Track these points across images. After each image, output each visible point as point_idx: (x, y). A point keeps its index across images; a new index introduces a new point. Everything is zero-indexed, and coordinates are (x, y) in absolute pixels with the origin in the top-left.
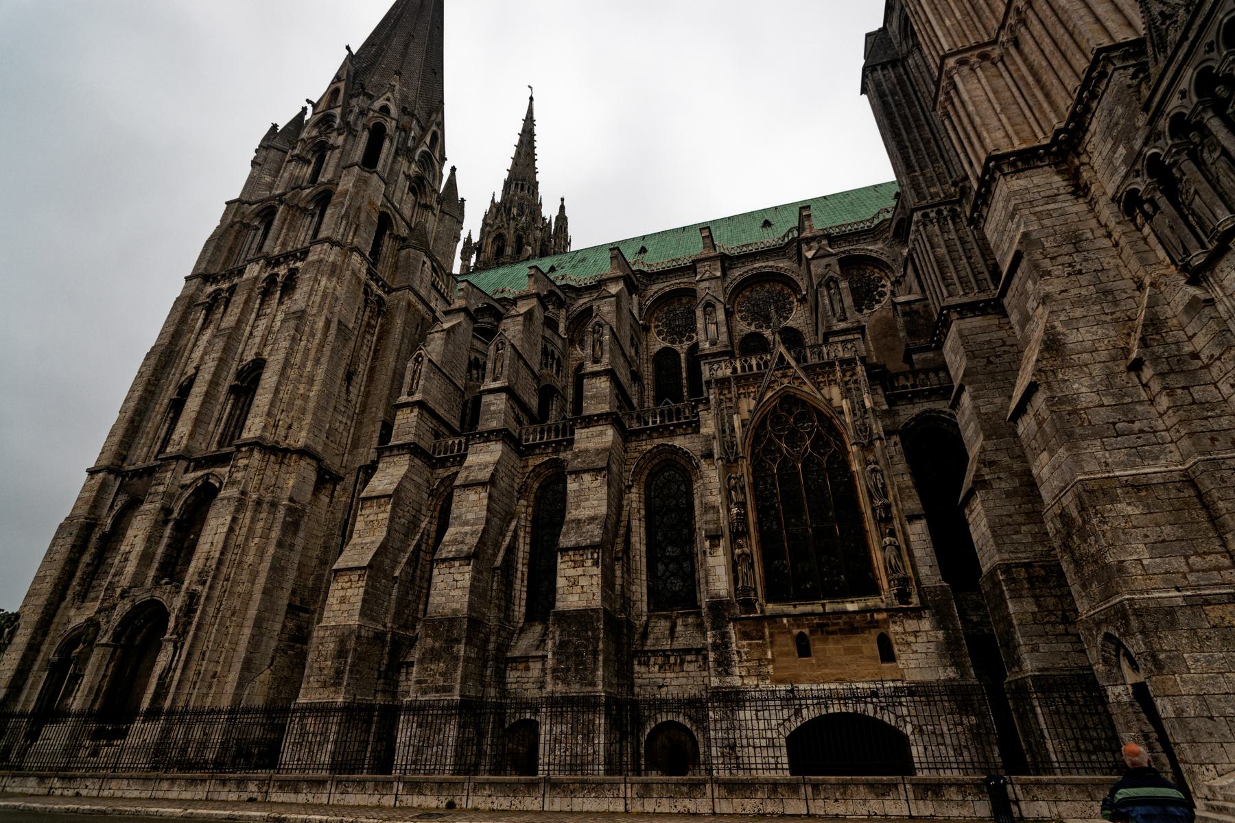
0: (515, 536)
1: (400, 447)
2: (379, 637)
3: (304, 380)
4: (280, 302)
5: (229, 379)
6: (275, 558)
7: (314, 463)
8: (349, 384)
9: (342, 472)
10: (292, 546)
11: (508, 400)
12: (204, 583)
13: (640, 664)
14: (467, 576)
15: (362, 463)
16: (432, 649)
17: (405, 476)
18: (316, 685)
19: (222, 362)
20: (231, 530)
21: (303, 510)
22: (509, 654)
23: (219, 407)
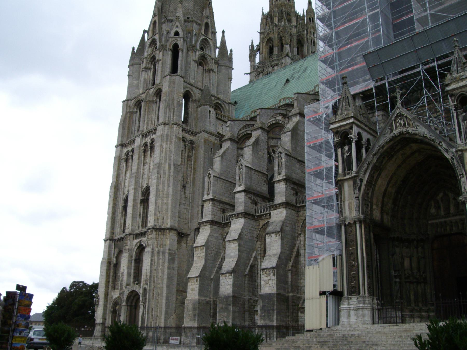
0: (256, 258)
1: (206, 222)
2: (208, 303)
3: (165, 196)
4: (151, 156)
5: (140, 197)
6: (168, 274)
7: (176, 232)
8: (185, 190)
9: (188, 232)
10: (173, 268)
11: (246, 195)
12: (147, 284)
13: (301, 313)
14: (232, 280)
15: (195, 228)
16: (222, 308)
17: (210, 235)
18: (188, 320)
19: (135, 189)
20: (151, 264)
21: (175, 253)
22: (255, 309)
23: (138, 210)
